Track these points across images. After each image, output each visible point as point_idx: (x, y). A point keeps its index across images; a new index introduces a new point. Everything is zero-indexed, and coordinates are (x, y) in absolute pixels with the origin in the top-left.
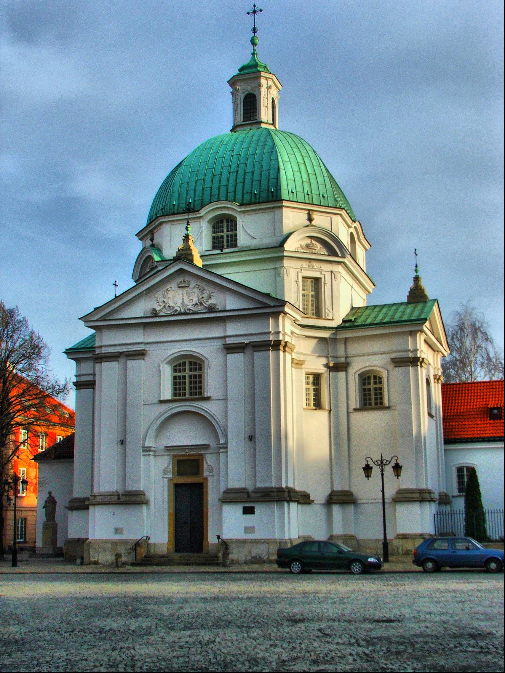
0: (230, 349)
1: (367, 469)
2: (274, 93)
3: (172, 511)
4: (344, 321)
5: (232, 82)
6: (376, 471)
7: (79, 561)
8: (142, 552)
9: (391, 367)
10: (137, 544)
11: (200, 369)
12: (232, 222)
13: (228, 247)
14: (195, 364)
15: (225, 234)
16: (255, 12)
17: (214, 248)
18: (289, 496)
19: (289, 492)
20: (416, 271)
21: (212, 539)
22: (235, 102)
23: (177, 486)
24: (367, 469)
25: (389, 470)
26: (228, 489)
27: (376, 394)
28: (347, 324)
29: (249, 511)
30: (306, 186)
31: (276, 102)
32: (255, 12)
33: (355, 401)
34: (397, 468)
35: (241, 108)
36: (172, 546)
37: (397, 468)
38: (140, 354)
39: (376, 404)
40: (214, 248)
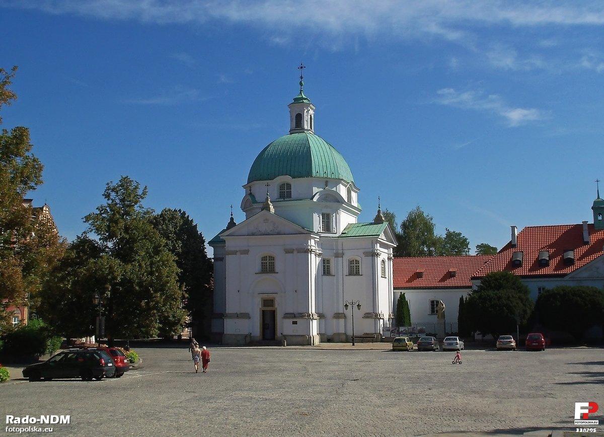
0: (288, 251)
1: (346, 306)
2: (311, 112)
3: (262, 322)
4: (342, 233)
5: (290, 106)
6: (350, 307)
7: (220, 343)
8: (248, 340)
9: (363, 256)
10: (246, 336)
11: (274, 260)
12: (289, 186)
13: (287, 197)
14: (272, 257)
15: (286, 190)
16: (302, 68)
17: (280, 197)
18: (312, 316)
19: (312, 315)
20: (379, 207)
21: (278, 334)
22: (291, 117)
23: (263, 311)
24: (346, 306)
25: (355, 306)
26: (286, 313)
27: (356, 269)
28: (344, 235)
29: (295, 323)
30: (325, 168)
31: (313, 116)
32: (302, 68)
33: (346, 271)
34: (359, 306)
35: (294, 121)
36: (261, 338)
37: (359, 306)
38: (246, 252)
39: (356, 273)
40: (280, 197)
